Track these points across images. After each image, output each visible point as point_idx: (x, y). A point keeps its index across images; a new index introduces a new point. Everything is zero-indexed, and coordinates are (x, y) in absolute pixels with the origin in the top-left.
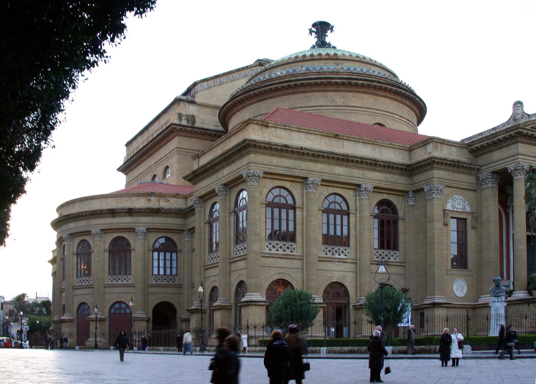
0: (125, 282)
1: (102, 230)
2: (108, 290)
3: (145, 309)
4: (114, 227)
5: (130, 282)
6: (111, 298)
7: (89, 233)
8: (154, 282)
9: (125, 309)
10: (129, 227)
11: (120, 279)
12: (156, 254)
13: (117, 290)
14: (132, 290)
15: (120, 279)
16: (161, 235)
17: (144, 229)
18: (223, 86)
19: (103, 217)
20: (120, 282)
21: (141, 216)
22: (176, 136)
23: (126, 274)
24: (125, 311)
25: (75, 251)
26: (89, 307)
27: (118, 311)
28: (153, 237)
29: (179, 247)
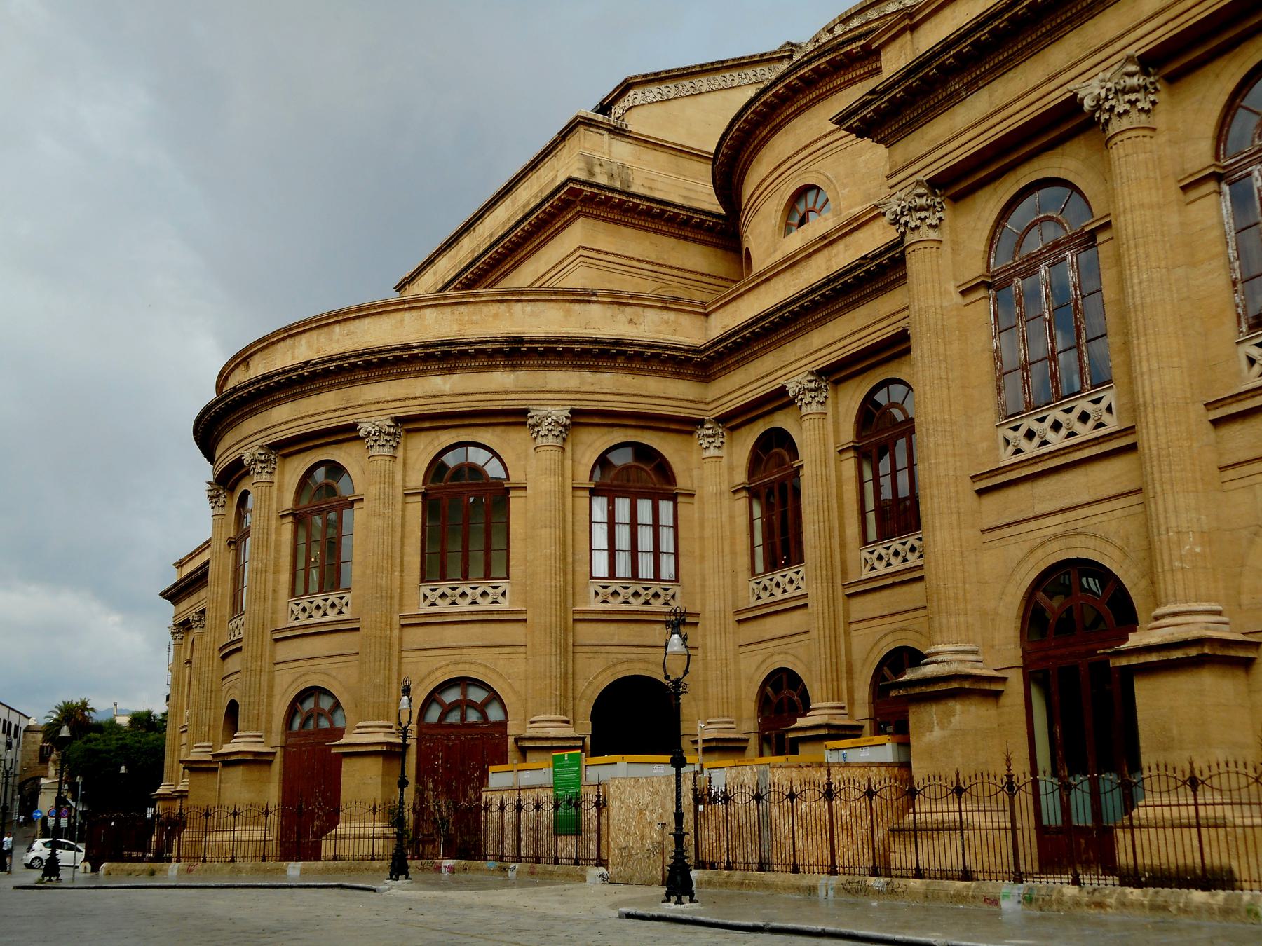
0: (484, 605)
1: (398, 420)
2: (415, 637)
3: (565, 703)
4: (448, 408)
5: (504, 604)
6: (428, 671)
7: (347, 434)
8: (595, 605)
9: (481, 708)
10: (506, 405)
11: (464, 595)
12: (600, 507)
13: (452, 635)
14: (514, 633)
15: (464, 595)
16: (619, 436)
17: (560, 413)
18: (700, 98)
19: (407, 375)
20: (464, 605)
21: (549, 367)
22: (578, 215)
23: (487, 576)
24: (485, 716)
25: (289, 503)
26: (337, 705)
27: (454, 717)
28: (594, 443)
29: (682, 483)
